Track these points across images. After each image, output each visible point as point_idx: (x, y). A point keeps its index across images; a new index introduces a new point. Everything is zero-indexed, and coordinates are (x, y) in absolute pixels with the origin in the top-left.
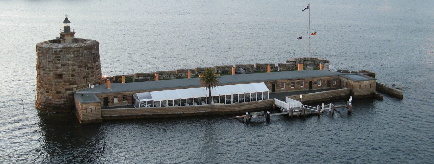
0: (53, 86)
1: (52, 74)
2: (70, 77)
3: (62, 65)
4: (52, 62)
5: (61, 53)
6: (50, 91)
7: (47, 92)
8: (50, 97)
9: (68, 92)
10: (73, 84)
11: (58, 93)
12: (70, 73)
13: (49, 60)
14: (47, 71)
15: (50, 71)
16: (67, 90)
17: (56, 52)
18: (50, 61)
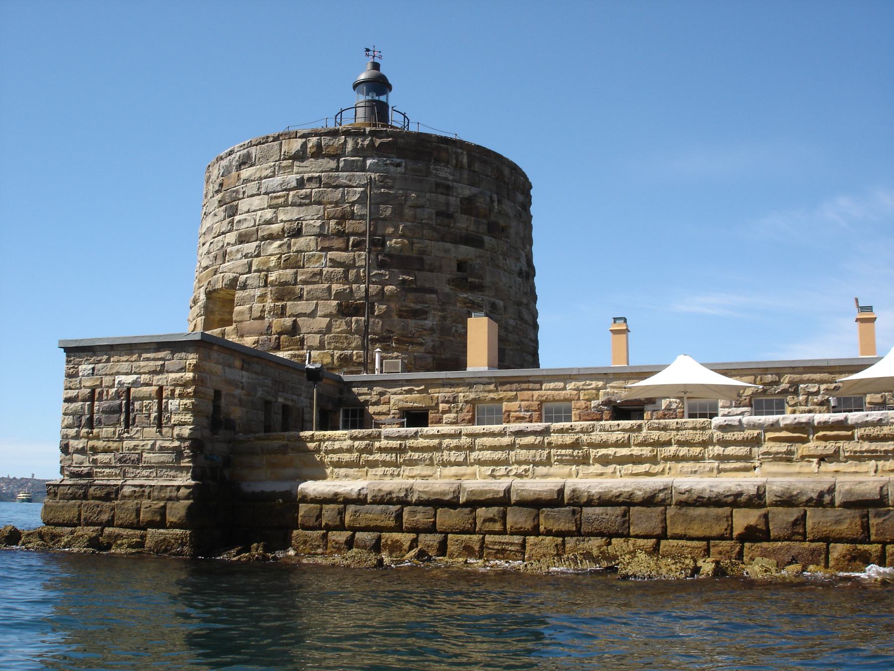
2: (269, 304)
3: (243, 239)
5: (246, 173)
12: (272, 277)
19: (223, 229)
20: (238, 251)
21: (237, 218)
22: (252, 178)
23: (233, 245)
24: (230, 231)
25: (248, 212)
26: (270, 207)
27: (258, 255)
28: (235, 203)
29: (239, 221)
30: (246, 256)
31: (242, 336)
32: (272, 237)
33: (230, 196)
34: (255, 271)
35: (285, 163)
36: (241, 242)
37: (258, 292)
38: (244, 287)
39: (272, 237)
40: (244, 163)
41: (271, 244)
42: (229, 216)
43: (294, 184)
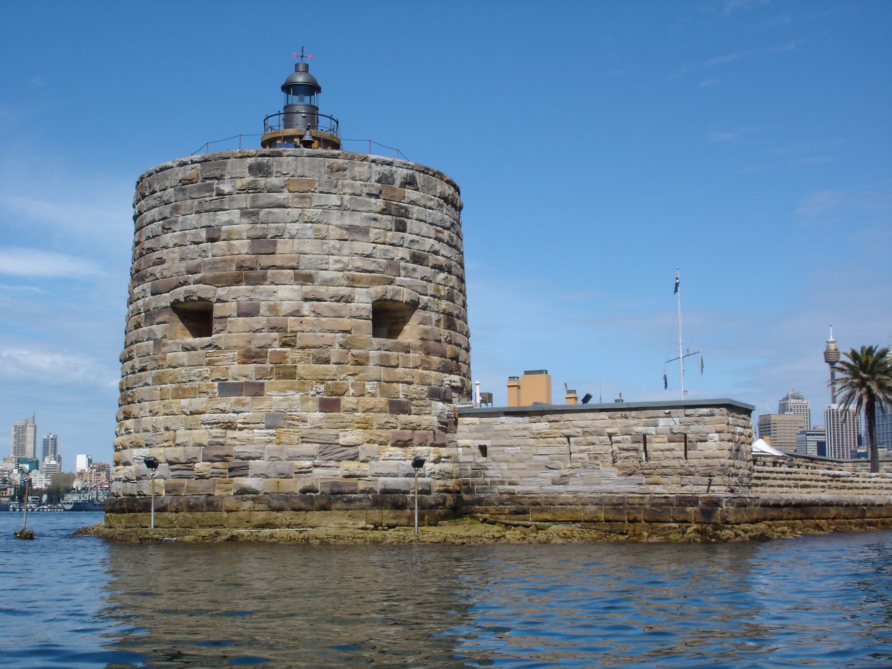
0: (372, 369)
1: (363, 300)
3: (418, 259)
4: (365, 231)
5: (411, 194)
6: (347, 401)
7: (329, 405)
8: (348, 437)
9: (439, 406)
10: (451, 372)
11: (398, 407)
12: (444, 304)
13: (347, 221)
14: (326, 283)
15: (353, 282)
16: (437, 394)
17: (385, 180)
18: (351, 229)
19: (395, 241)
20: (414, 270)
21: (408, 237)
22: (419, 203)
23: (407, 262)
24: (401, 246)
25: (418, 235)
26: (436, 239)
27: (431, 281)
28: (406, 220)
29: (412, 241)
30: (422, 279)
31: (428, 354)
32: (439, 268)
33: (398, 209)
34: (431, 296)
35: (441, 201)
36: (415, 262)
37: (434, 317)
38: (425, 308)
39: (439, 268)
40: (410, 184)
41: (438, 273)
42: (397, 230)
43: (448, 224)
